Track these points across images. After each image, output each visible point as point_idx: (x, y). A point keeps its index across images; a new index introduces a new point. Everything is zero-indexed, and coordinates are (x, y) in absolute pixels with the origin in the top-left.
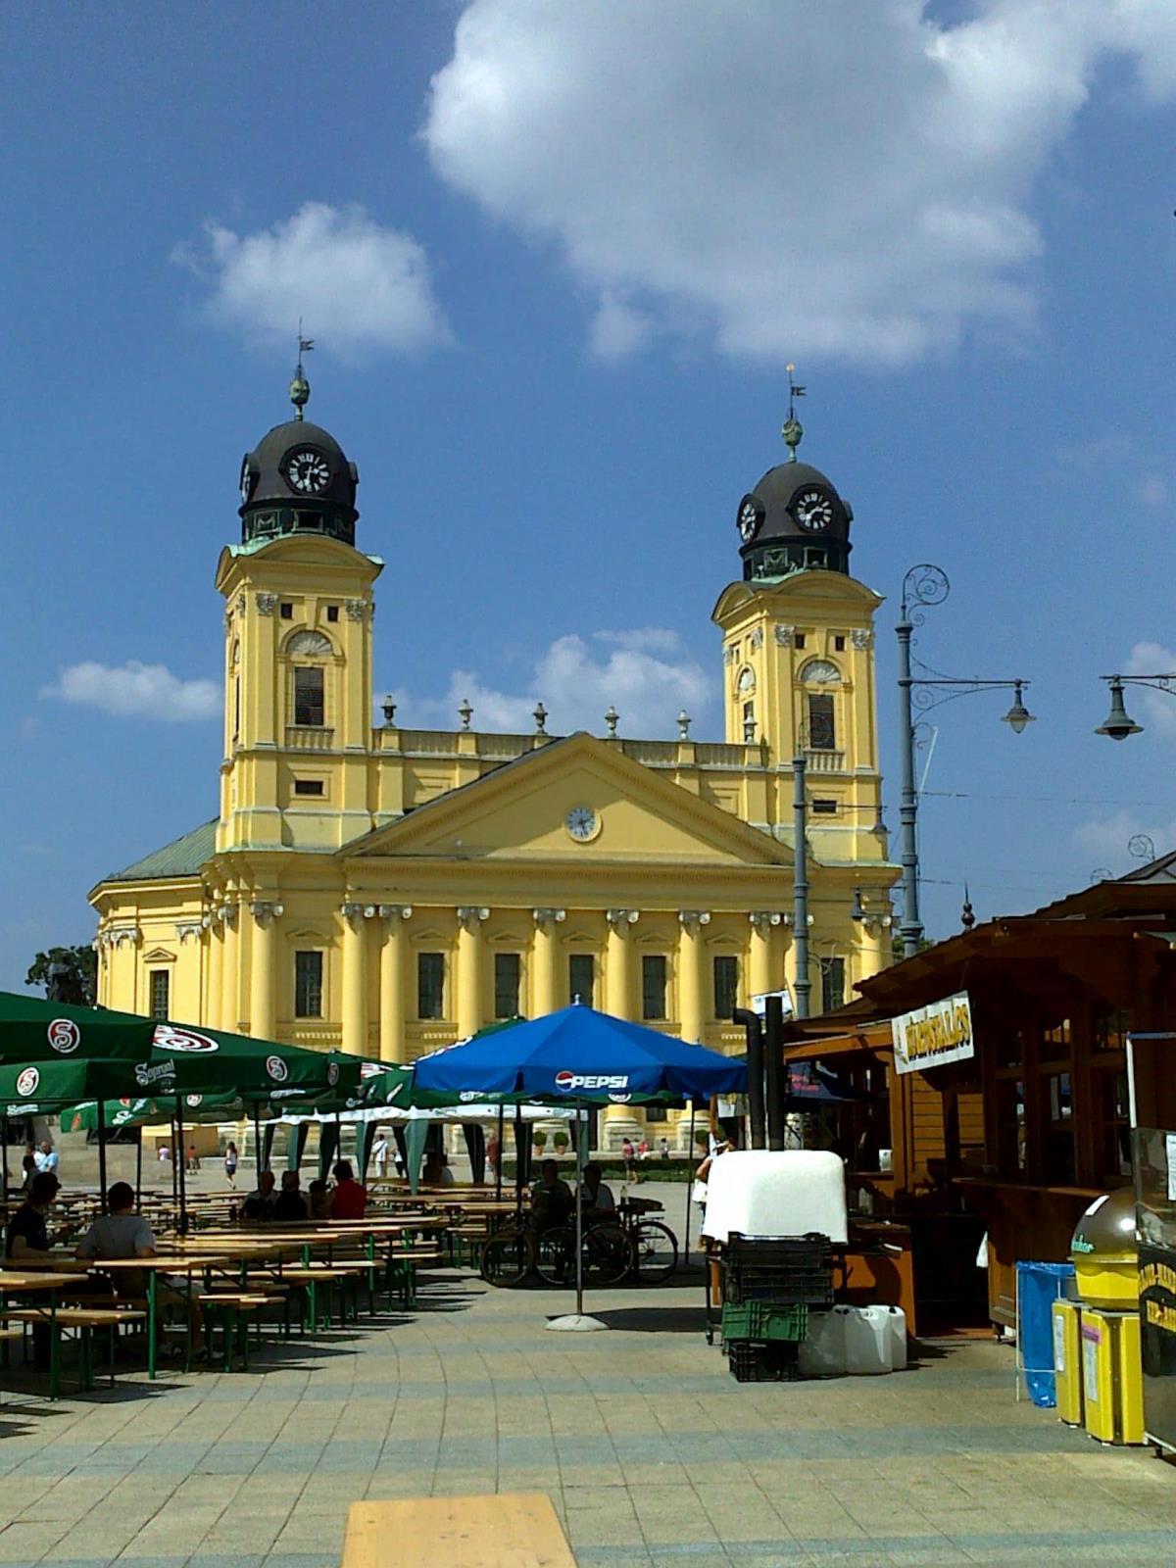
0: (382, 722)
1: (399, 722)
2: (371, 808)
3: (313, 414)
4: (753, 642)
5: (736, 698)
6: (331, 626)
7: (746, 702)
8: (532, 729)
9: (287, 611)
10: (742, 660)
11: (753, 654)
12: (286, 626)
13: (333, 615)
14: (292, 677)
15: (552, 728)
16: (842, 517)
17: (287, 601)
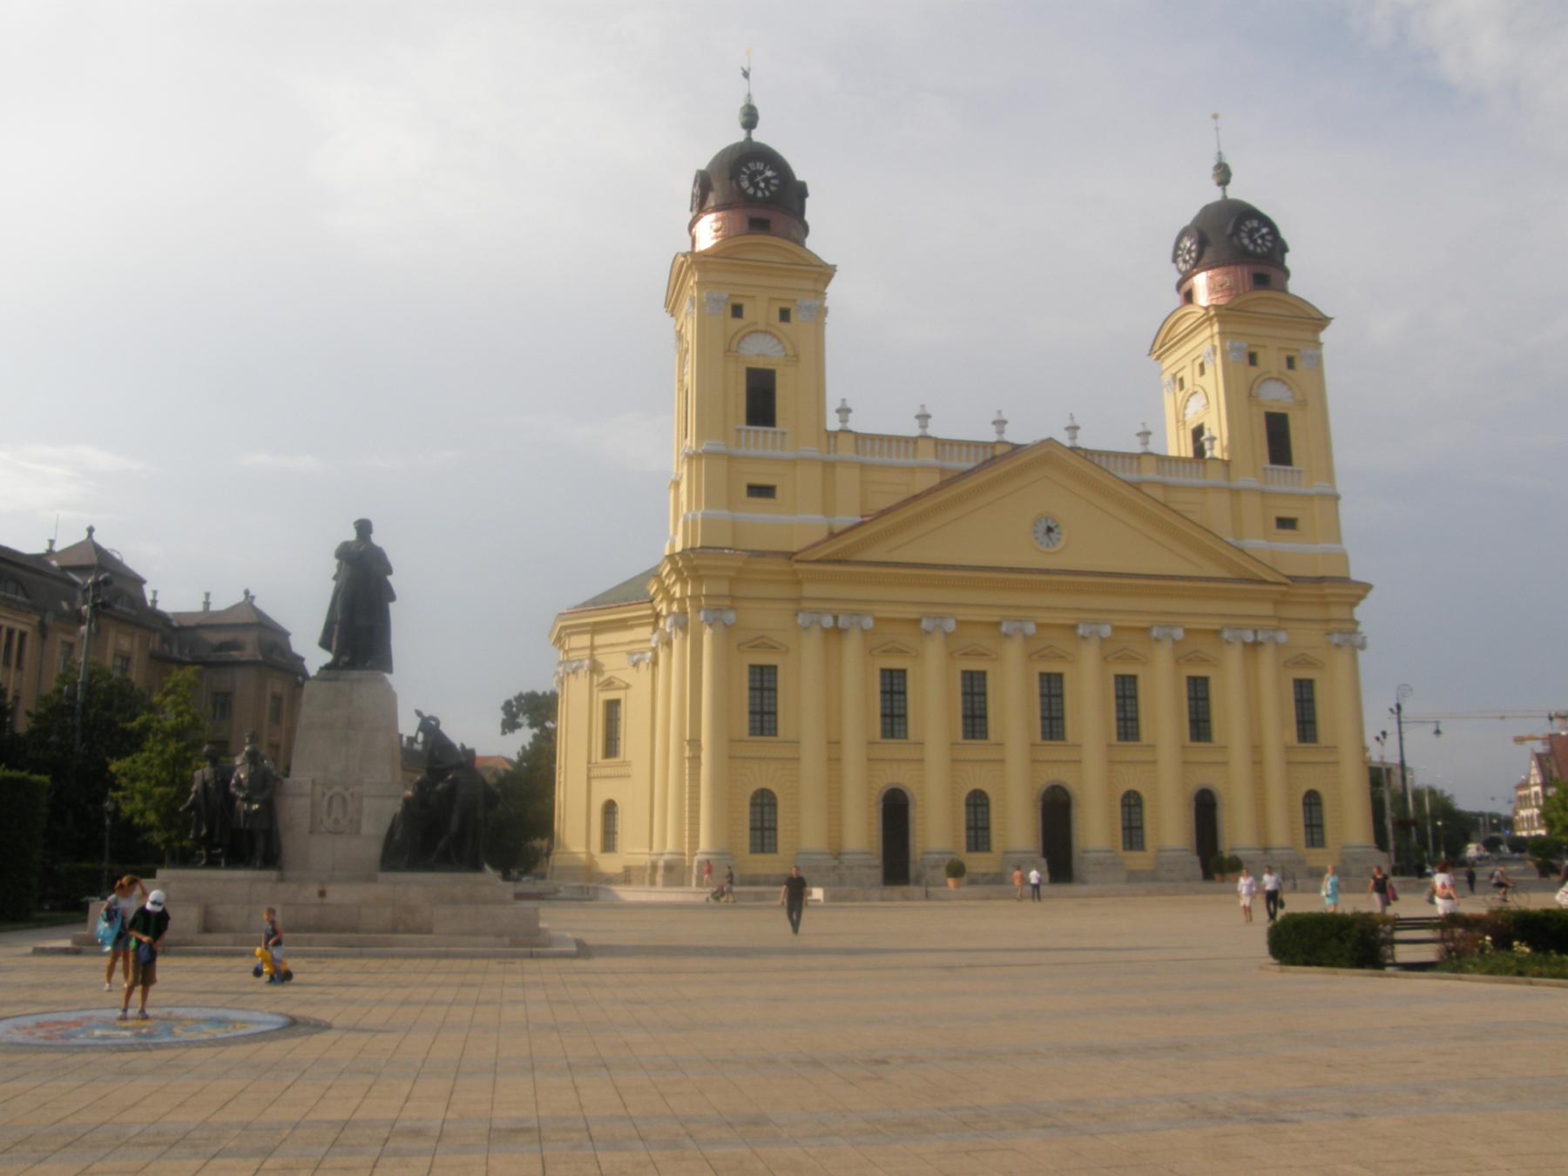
0: (833, 423)
1: (857, 424)
2: (827, 509)
3: (758, 136)
4: (1202, 365)
5: (1180, 420)
6: (784, 325)
7: (1194, 425)
8: (990, 436)
9: (737, 311)
10: (1187, 383)
11: (1202, 372)
12: (738, 323)
13: (785, 315)
14: (743, 379)
15: (1014, 435)
16: (1279, 248)
17: (738, 301)
